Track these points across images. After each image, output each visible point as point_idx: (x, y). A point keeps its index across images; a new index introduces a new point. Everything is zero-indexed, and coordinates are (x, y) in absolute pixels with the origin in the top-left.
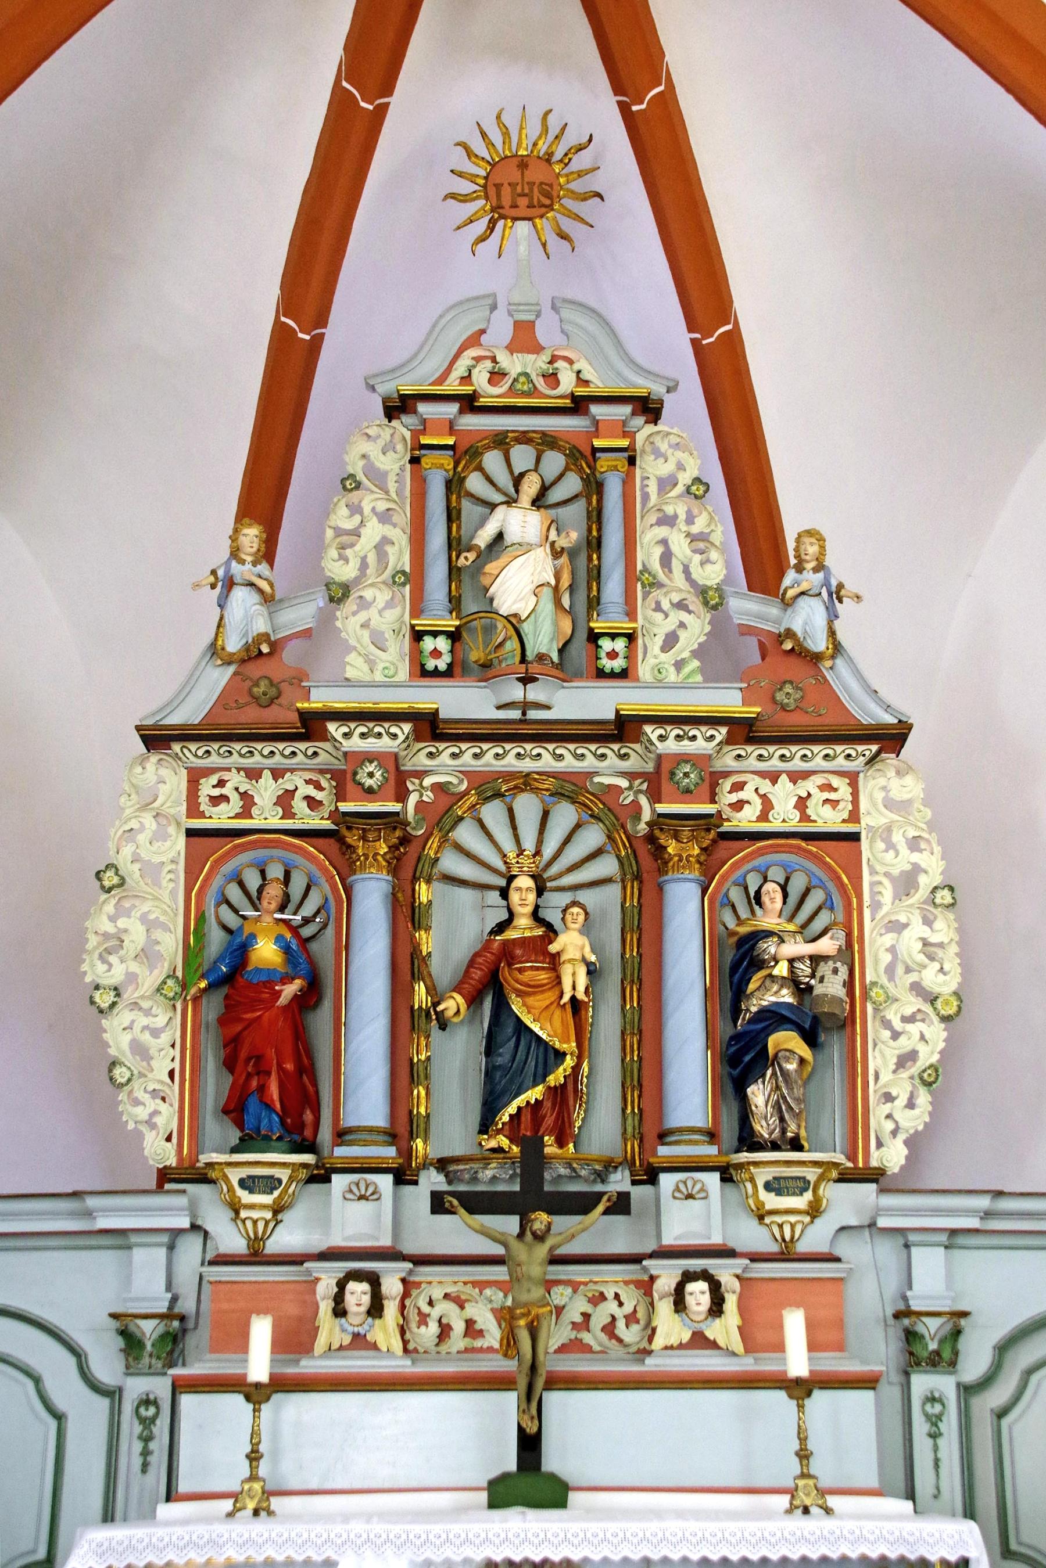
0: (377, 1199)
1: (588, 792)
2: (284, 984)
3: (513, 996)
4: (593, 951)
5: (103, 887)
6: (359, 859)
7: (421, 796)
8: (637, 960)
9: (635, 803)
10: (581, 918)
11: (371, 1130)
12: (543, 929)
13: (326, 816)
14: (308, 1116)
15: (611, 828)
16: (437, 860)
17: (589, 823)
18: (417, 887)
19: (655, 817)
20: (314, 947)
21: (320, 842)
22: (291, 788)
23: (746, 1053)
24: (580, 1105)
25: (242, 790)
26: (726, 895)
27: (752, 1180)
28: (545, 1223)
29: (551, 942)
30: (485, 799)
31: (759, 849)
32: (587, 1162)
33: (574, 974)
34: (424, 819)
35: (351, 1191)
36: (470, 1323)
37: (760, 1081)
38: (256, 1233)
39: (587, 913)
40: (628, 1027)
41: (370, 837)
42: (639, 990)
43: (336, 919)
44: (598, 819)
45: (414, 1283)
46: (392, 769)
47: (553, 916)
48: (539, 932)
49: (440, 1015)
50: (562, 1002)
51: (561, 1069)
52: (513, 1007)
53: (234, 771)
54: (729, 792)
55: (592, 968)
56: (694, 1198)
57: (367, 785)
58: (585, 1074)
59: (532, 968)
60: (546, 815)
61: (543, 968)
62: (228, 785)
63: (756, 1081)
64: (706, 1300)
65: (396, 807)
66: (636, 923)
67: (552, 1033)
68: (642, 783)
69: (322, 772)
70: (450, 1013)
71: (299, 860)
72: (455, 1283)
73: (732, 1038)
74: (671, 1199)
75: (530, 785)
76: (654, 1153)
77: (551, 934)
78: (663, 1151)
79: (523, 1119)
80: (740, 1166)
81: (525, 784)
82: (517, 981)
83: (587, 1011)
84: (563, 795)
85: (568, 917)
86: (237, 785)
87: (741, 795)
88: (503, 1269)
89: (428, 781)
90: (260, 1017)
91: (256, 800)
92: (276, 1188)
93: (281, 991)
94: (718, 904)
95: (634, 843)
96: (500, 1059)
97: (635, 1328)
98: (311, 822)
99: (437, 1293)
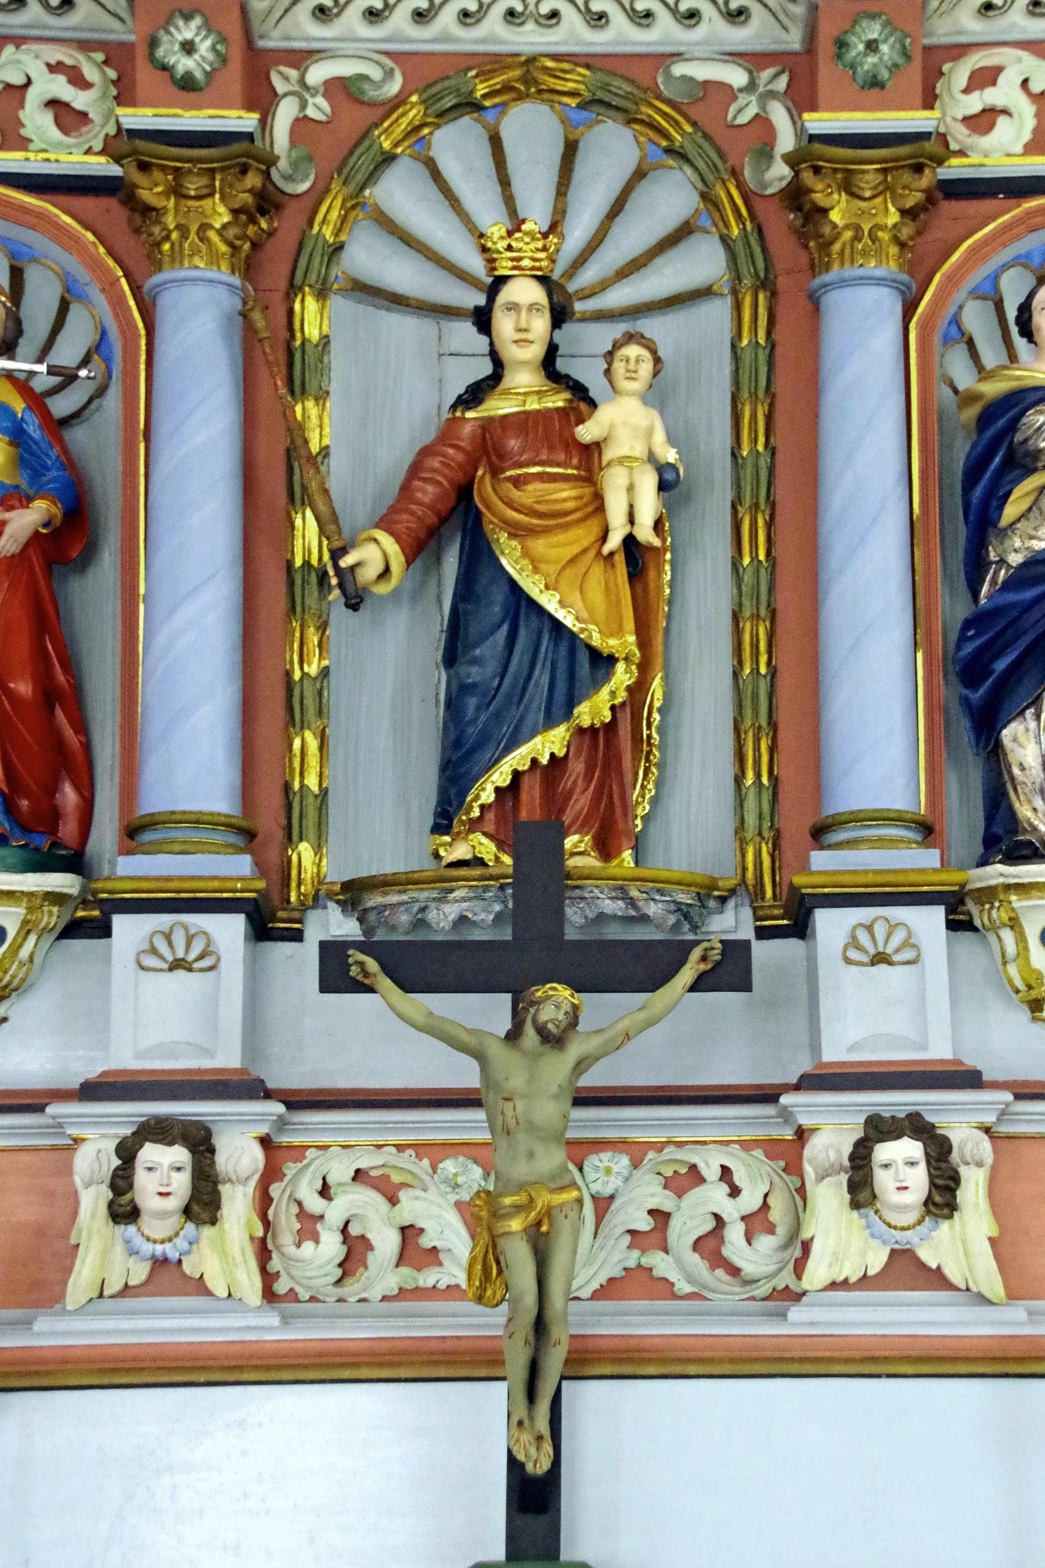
0: (211, 969)
1: (659, 97)
2: (11, 508)
3: (503, 537)
4: (672, 440)
6: (167, 238)
7: (303, 105)
8: (764, 462)
9: (762, 121)
10: (646, 368)
11: (198, 821)
12: (567, 395)
13: (98, 146)
14: (69, 795)
15: (710, 177)
16: (339, 248)
17: (663, 167)
18: (297, 306)
19: (806, 139)
20: (77, 436)
21: (87, 204)
22: (18, 80)
23: (998, 656)
24: (647, 771)
26: (956, 320)
27: (1014, 924)
28: (566, 1007)
29: (581, 421)
30: (440, 115)
31: (1031, 214)
32: (660, 886)
33: (631, 488)
34: (309, 158)
35: (154, 951)
36: (409, 1233)
37: (1030, 713)
39: (657, 360)
40: (746, 602)
41: (192, 187)
42: (769, 525)
43: (125, 372)
44: (682, 156)
45: (290, 1147)
46: (235, 32)
47: (589, 374)
48: (558, 400)
49: (346, 576)
50: (607, 549)
51: (605, 692)
52: (504, 562)
54: (966, 91)
55: (669, 476)
56: (890, 963)
57: (180, 70)
58: (657, 704)
59: (541, 477)
60: (571, 149)
61: (565, 478)
63: (1022, 713)
64: (919, 1179)
65: (246, 121)
66: (763, 382)
67: (585, 615)
68: (776, 76)
69: (85, 46)
70: (369, 573)
71: (36, 240)
72: (379, 1147)
73: (967, 624)
74: (843, 963)
75: (536, 82)
76: (804, 866)
77: (583, 407)
78: (821, 860)
79: (524, 796)
80: (988, 895)
81: (527, 80)
82: (510, 504)
83: (660, 572)
84: (608, 105)
85: (619, 367)
87: (992, 96)
88: (479, 1115)
89: (318, 73)
94: (937, 339)
95: (759, 206)
96: (474, 670)
97: (766, 1243)
98: (63, 158)
99: (340, 1170)
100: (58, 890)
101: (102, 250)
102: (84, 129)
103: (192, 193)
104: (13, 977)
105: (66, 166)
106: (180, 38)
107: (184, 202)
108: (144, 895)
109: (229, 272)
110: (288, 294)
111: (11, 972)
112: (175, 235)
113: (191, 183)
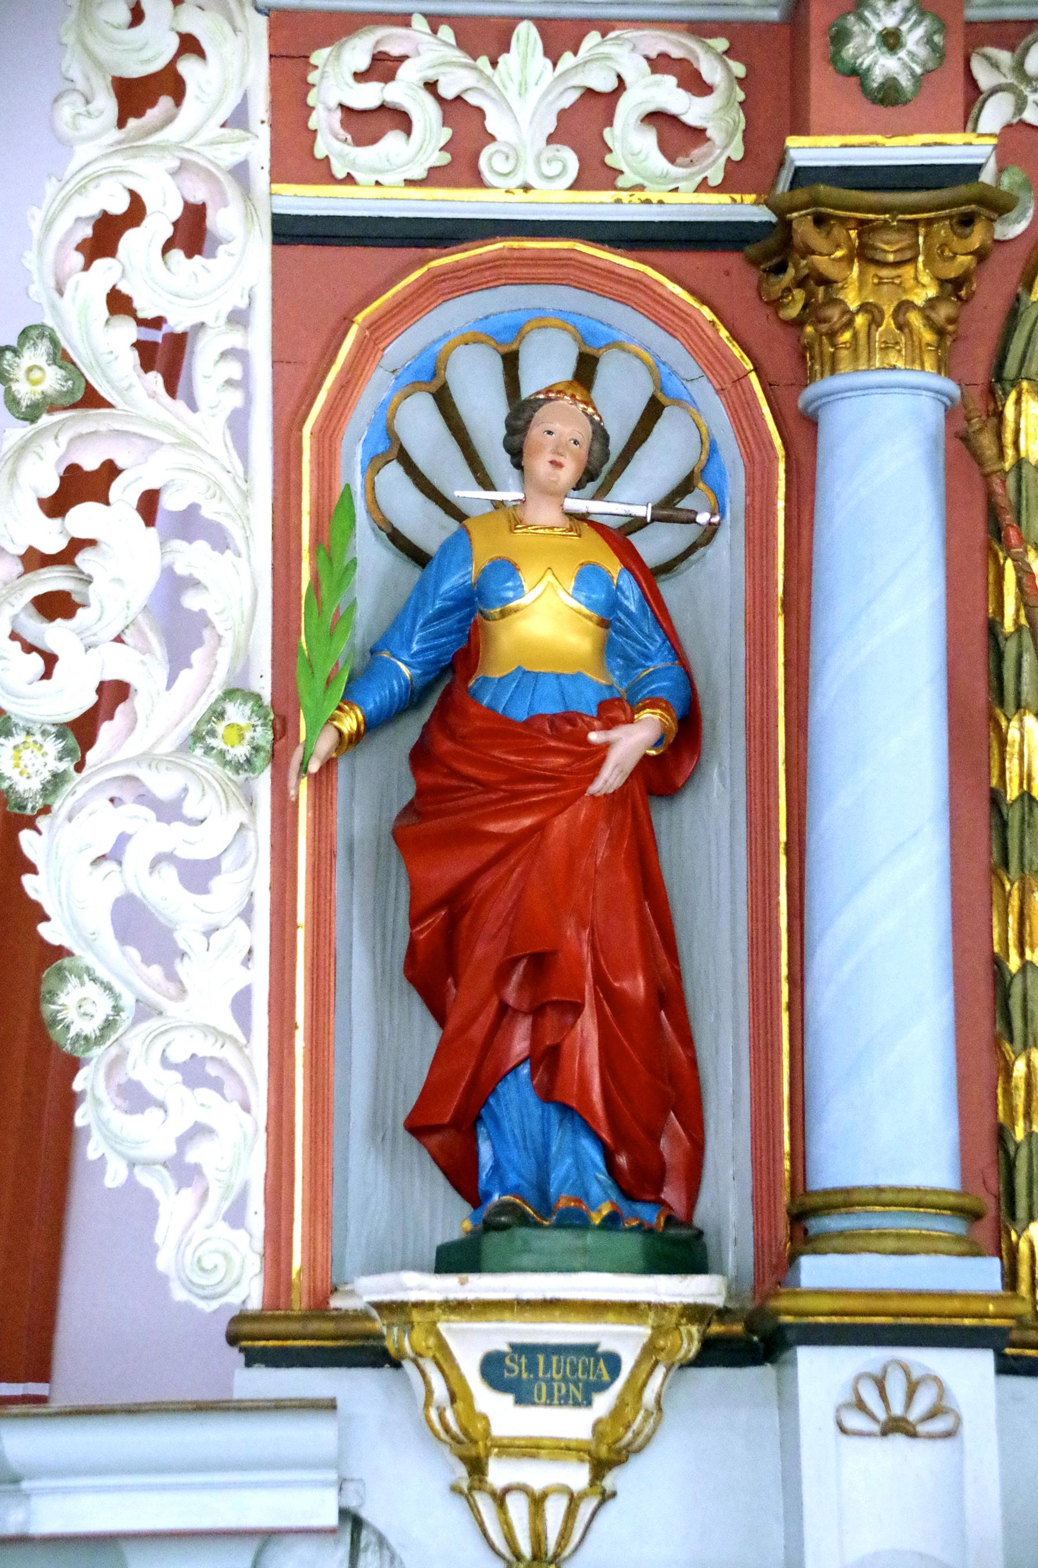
5: (12, 401)
6: (850, 324)
13: (716, 177)
22: (605, 84)
25: (448, 92)
38: (538, 1538)
41: (889, 247)
53: (419, 23)
62: (404, 71)
86: (431, 75)
90: (539, 828)
91: (492, 125)
92: (602, 1387)
93: (604, 749)
100: (700, 1300)
101: (724, 333)
102: (696, 153)
103: (891, 258)
104: (637, 1434)
105: (675, 208)
106: (878, 27)
107: (872, 270)
108: (847, 1320)
109: (935, 371)
110: (991, 392)
111: (635, 1426)
112: (860, 320)
113: (888, 243)
